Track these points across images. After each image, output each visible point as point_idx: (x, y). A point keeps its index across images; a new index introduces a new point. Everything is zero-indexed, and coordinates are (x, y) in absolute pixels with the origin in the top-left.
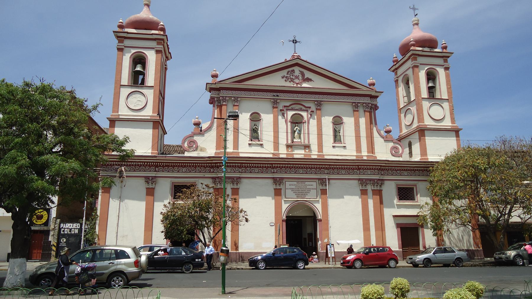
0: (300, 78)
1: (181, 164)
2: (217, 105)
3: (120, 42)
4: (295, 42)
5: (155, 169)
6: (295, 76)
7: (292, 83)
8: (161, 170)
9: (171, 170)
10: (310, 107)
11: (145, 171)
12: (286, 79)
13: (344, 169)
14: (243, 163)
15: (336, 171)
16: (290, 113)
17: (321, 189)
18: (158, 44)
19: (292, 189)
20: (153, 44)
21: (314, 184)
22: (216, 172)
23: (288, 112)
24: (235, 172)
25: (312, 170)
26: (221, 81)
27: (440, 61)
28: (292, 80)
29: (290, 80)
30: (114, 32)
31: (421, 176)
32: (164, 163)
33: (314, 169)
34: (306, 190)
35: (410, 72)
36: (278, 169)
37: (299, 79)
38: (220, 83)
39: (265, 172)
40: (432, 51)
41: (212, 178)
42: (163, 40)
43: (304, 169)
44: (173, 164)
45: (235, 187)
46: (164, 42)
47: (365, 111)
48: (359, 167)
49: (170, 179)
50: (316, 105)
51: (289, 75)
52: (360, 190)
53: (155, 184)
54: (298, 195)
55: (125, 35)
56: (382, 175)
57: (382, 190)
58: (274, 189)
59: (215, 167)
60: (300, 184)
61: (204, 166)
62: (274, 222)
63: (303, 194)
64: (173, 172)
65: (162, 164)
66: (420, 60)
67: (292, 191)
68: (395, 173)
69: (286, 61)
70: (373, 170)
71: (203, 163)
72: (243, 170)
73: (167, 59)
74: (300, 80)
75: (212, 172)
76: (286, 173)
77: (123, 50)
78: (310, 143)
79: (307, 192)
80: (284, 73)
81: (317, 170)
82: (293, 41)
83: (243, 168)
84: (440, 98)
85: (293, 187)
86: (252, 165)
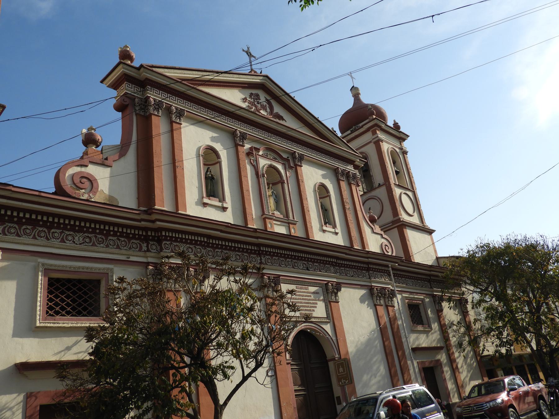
0: (268, 110)
2: (136, 114)
6: (261, 105)
10: (287, 160)
16: (263, 163)
22: (155, 251)
25: (315, 264)
26: (153, 67)
32: (25, 211)
33: (317, 262)
34: (312, 302)
35: (371, 150)
38: (149, 68)
41: (148, 264)
43: (304, 262)
47: (350, 184)
49: (41, 260)
50: (294, 158)
59: (152, 240)
61: (127, 236)
63: (308, 308)
65: (18, 214)
72: (210, 253)
75: (145, 251)
78: (295, 220)
79: (313, 305)
83: (209, 249)
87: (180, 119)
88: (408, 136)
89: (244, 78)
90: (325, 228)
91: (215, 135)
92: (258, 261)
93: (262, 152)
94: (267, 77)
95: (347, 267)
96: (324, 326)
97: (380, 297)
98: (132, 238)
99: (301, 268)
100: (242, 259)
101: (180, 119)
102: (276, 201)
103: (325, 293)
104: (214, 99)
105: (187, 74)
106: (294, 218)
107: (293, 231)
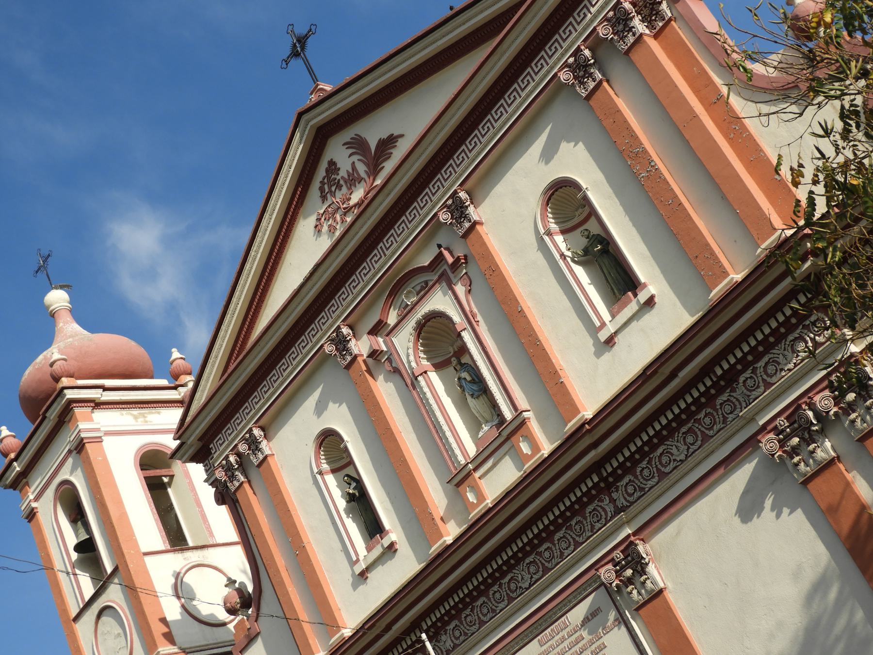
0: (362, 168)
6: (346, 182)
12: (329, 223)
15: (646, 473)
25: (556, 537)
28: (345, 206)
37: (361, 180)
38: (183, 428)
43: (527, 561)
48: (719, 372)
51: (328, 195)
55: (17, 467)
76: (482, 623)
77: (35, 514)
81: (573, 522)
82: (295, 54)
89: (279, 196)
90: (603, 336)
91: (316, 395)
92: (444, 650)
93: (394, 309)
94: (300, 115)
95: (654, 448)
99: (527, 585)
101: (260, 450)
102: (476, 394)
104: (262, 343)
105: (219, 352)
106: (515, 408)
107: (525, 448)
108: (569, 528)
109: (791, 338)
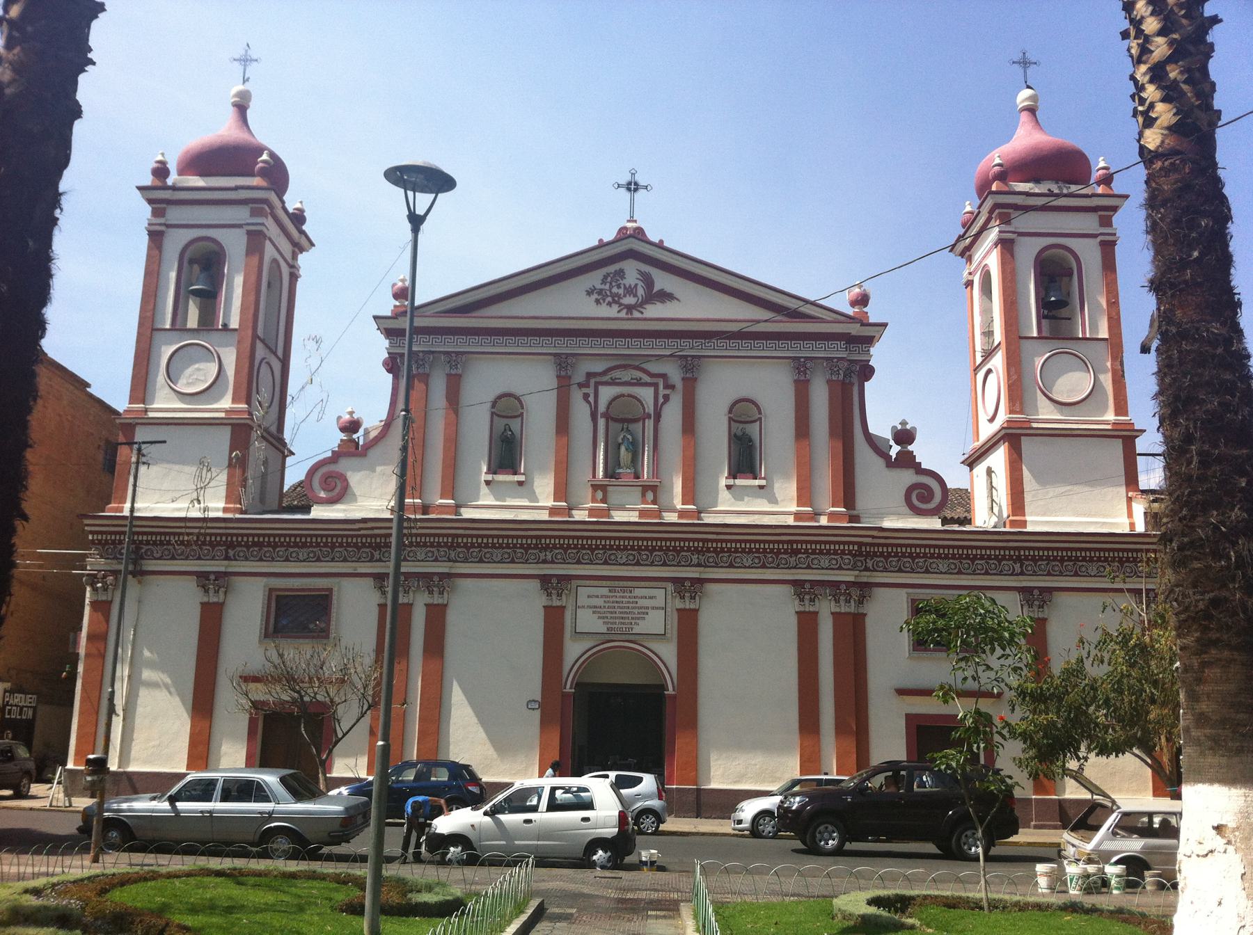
0: (641, 292)
1: (293, 539)
3: (156, 213)
4: (633, 187)
5: (227, 553)
6: (625, 287)
7: (615, 307)
8: (242, 554)
9: (268, 555)
10: (664, 376)
11: (199, 558)
13: (748, 553)
14: (457, 536)
15: (725, 559)
16: (606, 393)
17: (677, 609)
18: (254, 213)
19: (595, 607)
20: (241, 214)
21: (660, 593)
23: (600, 387)
24: (436, 560)
27: (1089, 223)
28: (616, 299)
29: (609, 299)
30: (140, 188)
31: (995, 574)
33: (658, 551)
36: (557, 551)
37: (635, 295)
39: (521, 560)
40: (1065, 191)
42: (265, 201)
44: (272, 539)
45: (437, 600)
46: (271, 207)
47: (829, 382)
48: (795, 546)
49: (265, 579)
52: (797, 612)
53: (225, 593)
54: (610, 626)
56: (867, 569)
57: (865, 615)
58: (544, 607)
60: (618, 594)
62: (540, 700)
63: (627, 621)
64: (273, 560)
66: (1024, 222)
67: (594, 612)
68: (907, 565)
69: (602, 245)
70: (838, 554)
71: (352, 536)
72: (461, 555)
73: (297, 250)
74: (640, 298)
75: (377, 561)
76: (578, 562)
80: (594, 279)
83: (460, 550)
84: (1080, 336)
85: (599, 602)
86: (485, 541)
87: (457, 368)
88: (1127, 197)
96: (655, 646)
97: (812, 600)
98: (361, 547)
100: (513, 558)
101: (457, 368)
103: (669, 597)
108: (666, 554)
109: (833, 557)
